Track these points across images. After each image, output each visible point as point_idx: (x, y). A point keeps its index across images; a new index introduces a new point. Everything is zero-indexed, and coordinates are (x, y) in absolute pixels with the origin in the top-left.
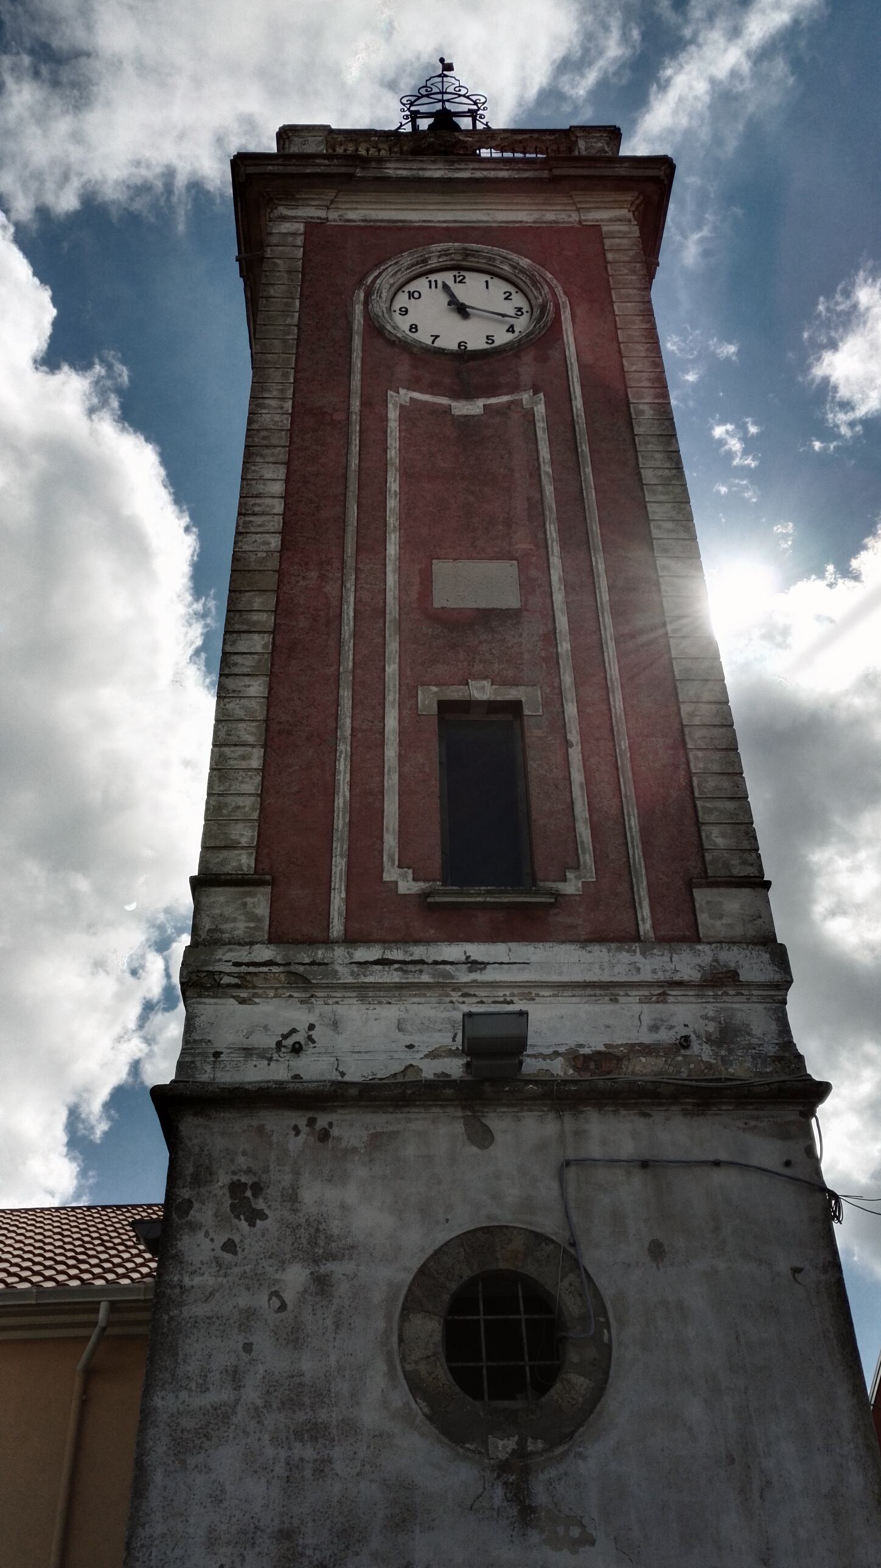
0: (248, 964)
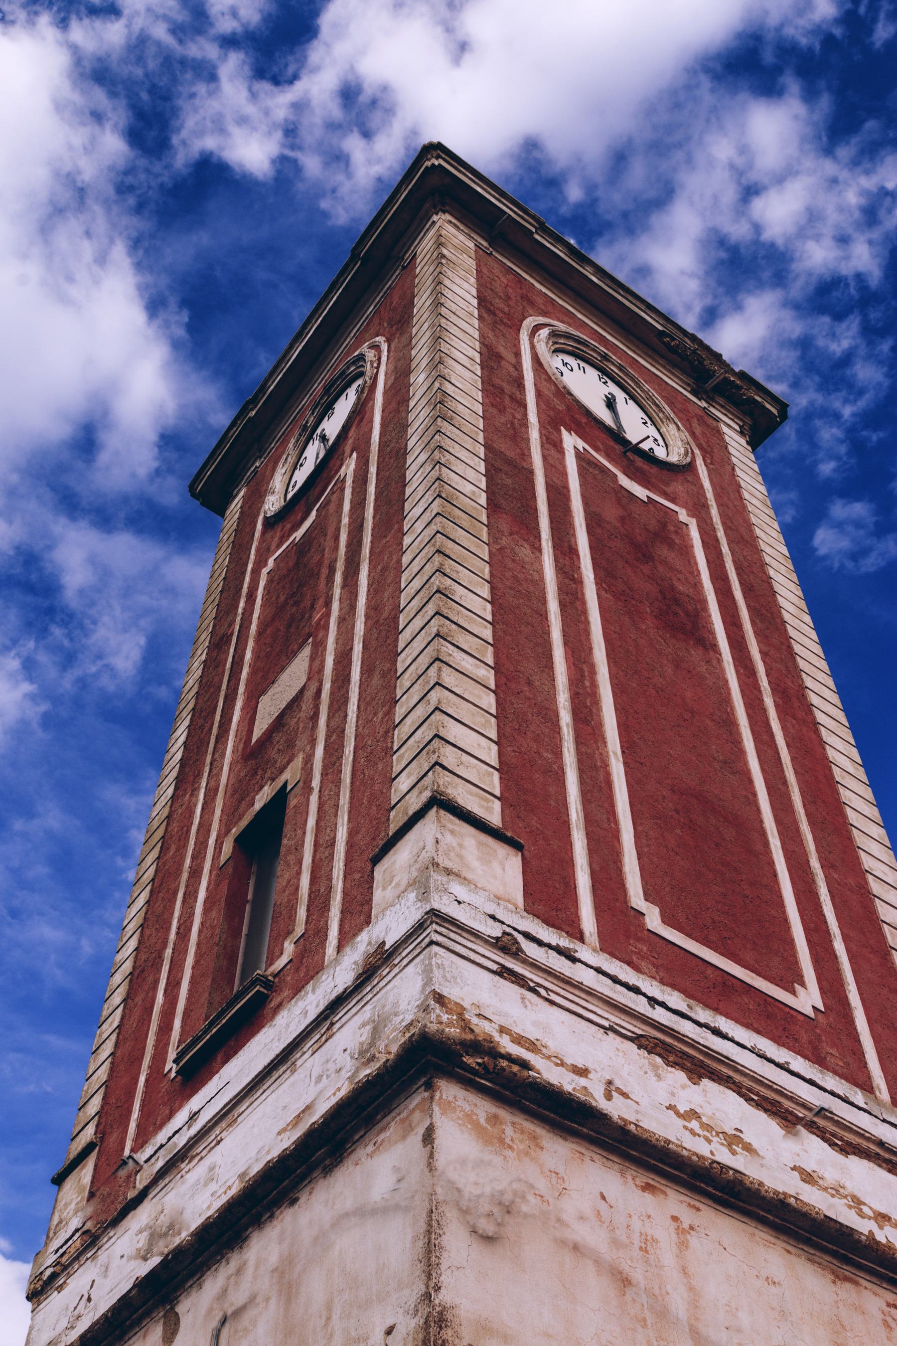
0: (61, 1247)
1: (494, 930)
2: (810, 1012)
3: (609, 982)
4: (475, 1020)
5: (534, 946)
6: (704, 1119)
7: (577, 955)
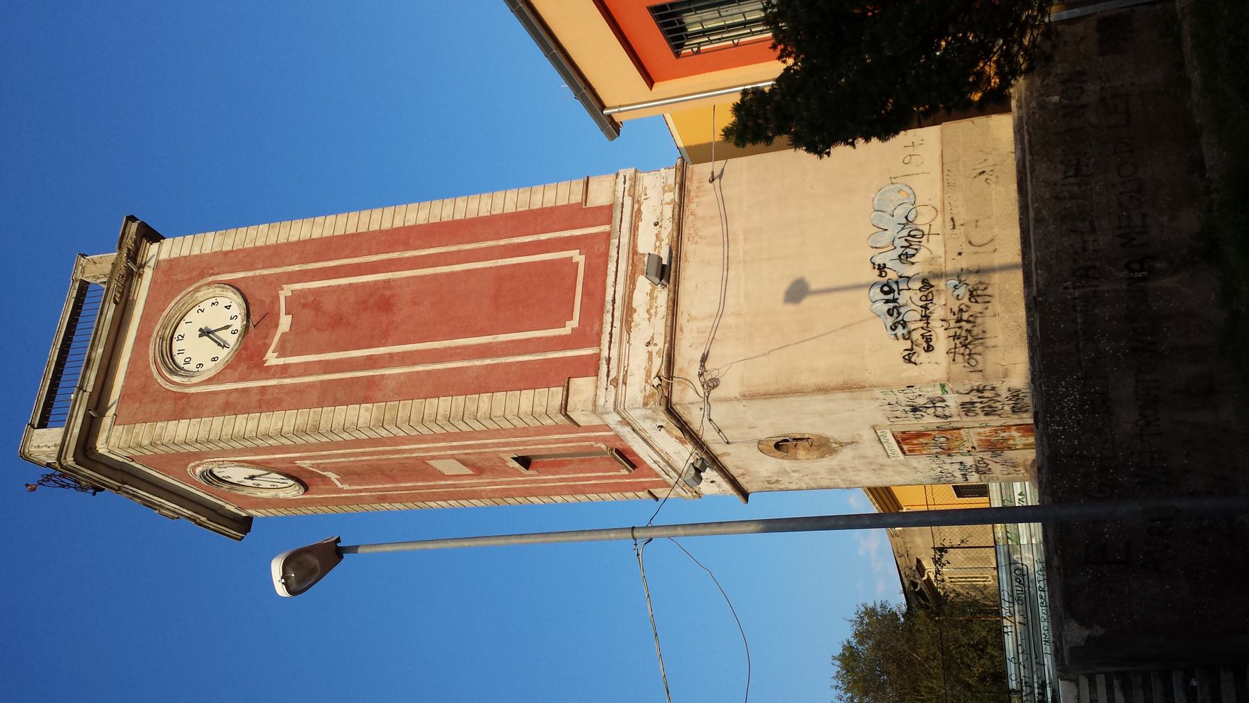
1: (611, 388)
2: (583, 257)
3: (612, 344)
4: (648, 392)
5: (611, 373)
6: (648, 307)
7: (607, 357)
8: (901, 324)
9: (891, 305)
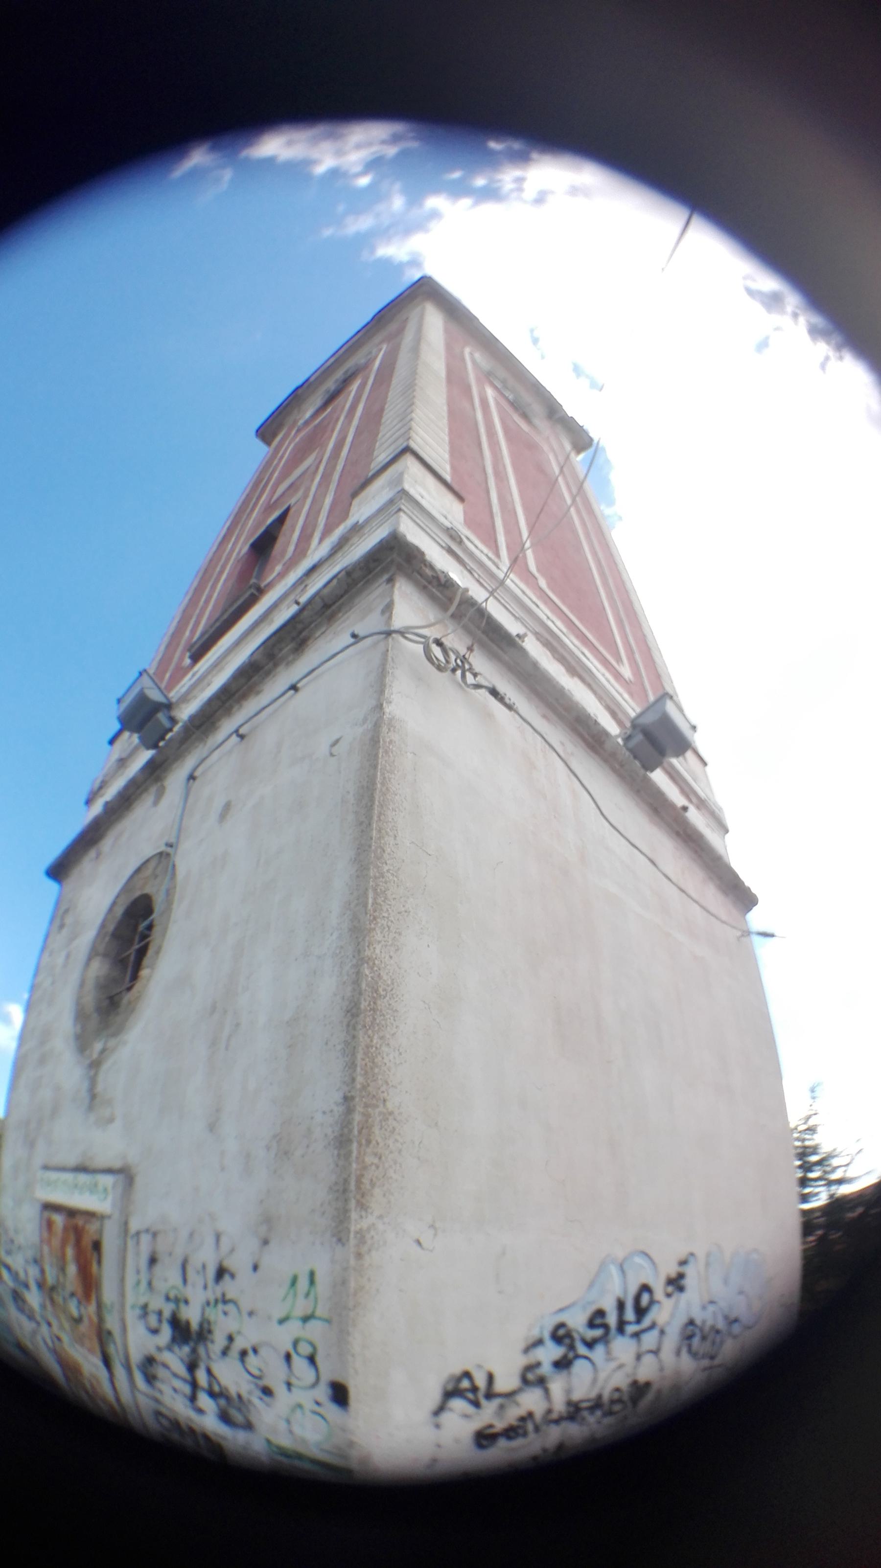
8: (565, 1357)
9: (612, 1319)
